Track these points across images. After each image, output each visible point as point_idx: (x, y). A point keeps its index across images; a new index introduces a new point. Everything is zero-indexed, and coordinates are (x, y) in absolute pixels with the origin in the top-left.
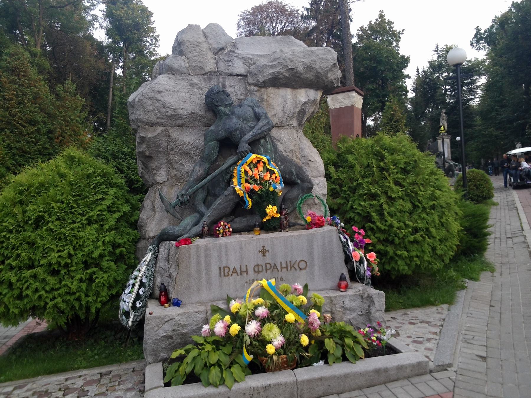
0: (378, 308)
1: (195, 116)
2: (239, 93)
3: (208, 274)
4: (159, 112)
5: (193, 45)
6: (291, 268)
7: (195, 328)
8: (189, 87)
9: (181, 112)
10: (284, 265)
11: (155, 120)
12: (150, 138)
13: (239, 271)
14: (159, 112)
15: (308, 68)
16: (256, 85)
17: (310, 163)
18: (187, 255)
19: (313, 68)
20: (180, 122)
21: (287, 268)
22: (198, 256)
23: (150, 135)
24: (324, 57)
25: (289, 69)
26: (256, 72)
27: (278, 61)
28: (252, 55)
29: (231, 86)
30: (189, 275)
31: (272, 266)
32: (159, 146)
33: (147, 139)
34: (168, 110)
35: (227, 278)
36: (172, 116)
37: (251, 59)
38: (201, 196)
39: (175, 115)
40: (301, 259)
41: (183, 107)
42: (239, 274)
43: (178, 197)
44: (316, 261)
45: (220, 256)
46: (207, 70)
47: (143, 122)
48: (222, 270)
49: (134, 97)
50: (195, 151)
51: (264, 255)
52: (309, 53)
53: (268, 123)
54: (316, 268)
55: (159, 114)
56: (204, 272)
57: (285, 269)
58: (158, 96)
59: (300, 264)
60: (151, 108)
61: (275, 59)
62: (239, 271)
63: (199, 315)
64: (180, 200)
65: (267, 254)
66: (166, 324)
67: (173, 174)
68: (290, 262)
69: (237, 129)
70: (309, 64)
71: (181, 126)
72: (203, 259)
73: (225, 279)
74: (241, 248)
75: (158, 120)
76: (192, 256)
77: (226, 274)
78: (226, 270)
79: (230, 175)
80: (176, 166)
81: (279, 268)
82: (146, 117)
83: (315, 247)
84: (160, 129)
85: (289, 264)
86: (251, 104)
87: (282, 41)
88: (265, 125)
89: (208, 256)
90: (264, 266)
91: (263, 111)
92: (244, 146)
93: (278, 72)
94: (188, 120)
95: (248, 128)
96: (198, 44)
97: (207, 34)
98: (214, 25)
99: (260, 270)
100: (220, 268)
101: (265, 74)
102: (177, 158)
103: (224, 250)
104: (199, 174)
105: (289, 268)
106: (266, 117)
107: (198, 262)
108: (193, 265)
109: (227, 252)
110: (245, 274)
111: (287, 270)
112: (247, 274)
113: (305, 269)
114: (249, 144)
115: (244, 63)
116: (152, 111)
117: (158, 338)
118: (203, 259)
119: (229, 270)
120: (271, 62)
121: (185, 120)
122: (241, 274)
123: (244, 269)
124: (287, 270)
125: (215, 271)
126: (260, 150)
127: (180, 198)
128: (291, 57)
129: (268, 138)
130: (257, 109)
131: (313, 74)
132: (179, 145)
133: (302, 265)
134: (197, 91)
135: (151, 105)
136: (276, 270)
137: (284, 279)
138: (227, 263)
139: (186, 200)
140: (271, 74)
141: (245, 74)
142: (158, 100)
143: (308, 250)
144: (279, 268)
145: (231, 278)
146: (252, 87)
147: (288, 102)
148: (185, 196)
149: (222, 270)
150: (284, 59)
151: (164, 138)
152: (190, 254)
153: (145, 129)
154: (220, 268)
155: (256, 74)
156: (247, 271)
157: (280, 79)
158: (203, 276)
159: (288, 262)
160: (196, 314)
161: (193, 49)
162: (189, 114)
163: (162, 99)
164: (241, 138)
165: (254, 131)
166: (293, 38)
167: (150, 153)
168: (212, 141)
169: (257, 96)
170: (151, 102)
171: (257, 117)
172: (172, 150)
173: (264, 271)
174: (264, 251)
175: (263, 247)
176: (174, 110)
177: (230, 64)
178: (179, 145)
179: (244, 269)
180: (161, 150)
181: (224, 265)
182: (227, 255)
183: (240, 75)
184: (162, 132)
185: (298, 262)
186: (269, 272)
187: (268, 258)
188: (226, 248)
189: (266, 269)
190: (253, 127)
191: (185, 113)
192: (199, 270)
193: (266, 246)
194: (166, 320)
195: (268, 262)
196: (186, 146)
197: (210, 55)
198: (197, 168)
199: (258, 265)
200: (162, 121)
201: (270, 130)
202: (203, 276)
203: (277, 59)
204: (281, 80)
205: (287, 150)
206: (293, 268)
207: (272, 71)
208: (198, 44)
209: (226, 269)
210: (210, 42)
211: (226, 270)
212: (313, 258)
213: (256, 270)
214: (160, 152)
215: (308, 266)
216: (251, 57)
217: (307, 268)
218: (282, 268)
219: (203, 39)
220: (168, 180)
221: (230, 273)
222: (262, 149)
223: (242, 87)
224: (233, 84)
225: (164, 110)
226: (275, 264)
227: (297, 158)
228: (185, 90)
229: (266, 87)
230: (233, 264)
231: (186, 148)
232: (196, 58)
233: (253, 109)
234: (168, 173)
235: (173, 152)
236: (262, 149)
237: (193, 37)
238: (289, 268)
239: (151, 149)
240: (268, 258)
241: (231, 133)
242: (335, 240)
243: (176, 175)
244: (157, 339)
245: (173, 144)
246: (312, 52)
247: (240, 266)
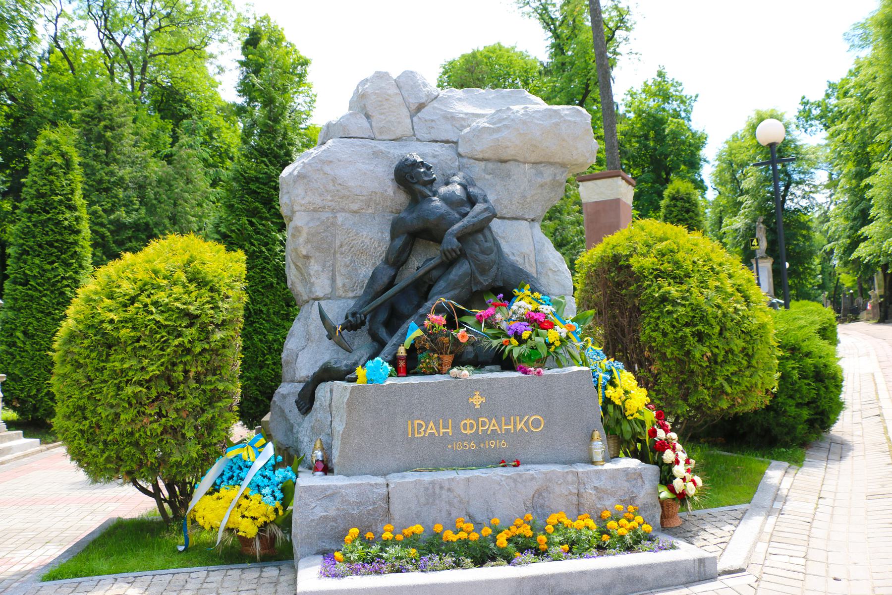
5: (380, 99)
7: (371, 508)
9: (358, 192)
11: (318, 201)
17: (550, 273)
20: (355, 207)
25: (520, 134)
27: (504, 123)
28: (466, 114)
34: (339, 187)
37: (463, 119)
38: (383, 316)
39: (349, 197)
43: (347, 317)
46: (399, 133)
49: (291, 170)
50: (375, 248)
53: (486, 210)
58: (327, 169)
61: (501, 120)
64: (350, 321)
69: (442, 217)
79: (427, 286)
84: (324, 216)
86: (464, 182)
87: (510, 97)
88: (482, 212)
91: (480, 192)
92: (451, 242)
95: (457, 216)
97: (402, 84)
98: (412, 72)
106: (485, 201)
114: (459, 239)
117: (316, 518)
120: (494, 124)
127: (350, 318)
128: (524, 118)
129: (486, 232)
130: (471, 189)
139: (359, 321)
141: (455, 140)
150: (513, 120)
157: (507, 147)
163: (330, 172)
164: (446, 231)
165: (466, 220)
166: (527, 93)
171: (471, 201)
177: (433, 124)
183: (447, 142)
184: (328, 218)
190: (466, 214)
191: (365, 193)
194: (328, 493)
196: (363, 242)
197: (405, 112)
201: (489, 219)
203: (504, 119)
205: (515, 252)
207: (495, 136)
210: (406, 95)
219: (393, 90)
227: (531, 265)
232: (383, 117)
244: (313, 521)
246: (555, 111)
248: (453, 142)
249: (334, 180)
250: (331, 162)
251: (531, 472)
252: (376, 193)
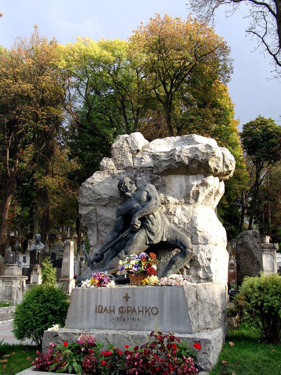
0: (204, 351)
1: (114, 199)
2: (145, 181)
3: (88, 310)
4: (91, 197)
6: (146, 312)
8: (112, 179)
9: (104, 196)
10: (141, 309)
11: (88, 202)
12: (84, 214)
13: (108, 310)
14: (91, 197)
15: (192, 160)
16: (158, 174)
18: (76, 295)
19: (196, 160)
20: (104, 203)
21: (143, 311)
22: (83, 296)
23: (85, 213)
24: (205, 151)
26: (157, 165)
28: (160, 152)
29: (140, 176)
30: (76, 308)
31: (132, 308)
32: (91, 220)
33: (83, 215)
35: (100, 314)
36: (99, 199)
37: (158, 156)
39: (101, 199)
40: (154, 306)
41: (106, 193)
42: (109, 312)
44: (165, 309)
45: (97, 298)
46: (126, 166)
47: (81, 204)
48: (98, 308)
51: (127, 300)
52: (194, 149)
54: (165, 314)
55: (91, 198)
56: (86, 308)
57: (142, 313)
59: (153, 309)
60: (86, 194)
62: (108, 310)
63: (74, 336)
65: (129, 300)
66: (55, 337)
67: (100, 239)
68: (146, 307)
70: (193, 158)
71: (105, 206)
72: (85, 299)
73: (99, 315)
74: (111, 294)
75: (90, 202)
76: (79, 295)
77: (100, 311)
78: (100, 308)
80: (102, 234)
81: (137, 311)
82: (83, 201)
83: (165, 298)
84: (91, 208)
85: (144, 309)
89: (89, 297)
90: (126, 308)
93: (170, 165)
94: (110, 201)
96: (121, 149)
99: (123, 311)
100: (96, 306)
101: (162, 167)
102: (103, 228)
103: (99, 294)
104: (110, 240)
105: (144, 312)
107: (83, 300)
108: (79, 302)
109: (101, 295)
110: (113, 312)
111: (143, 314)
112: (114, 313)
113: (156, 314)
115: (153, 159)
116: (86, 196)
118: (85, 299)
119: (102, 309)
121: (107, 202)
122: (110, 313)
123: (112, 309)
124: (143, 314)
125: (93, 308)
126: (148, 223)
131: (197, 165)
132: (104, 219)
133: (155, 311)
134: (116, 181)
135: (86, 192)
136: (134, 313)
137: (140, 320)
138: (101, 303)
140: (166, 166)
141: (153, 166)
142: (90, 189)
143: (159, 299)
144: (137, 311)
145: (104, 314)
146: (156, 176)
147: (183, 185)
148: (98, 255)
149: (98, 308)
151: (94, 215)
152: (78, 295)
153: (82, 208)
154: (96, 306)
155: (158, 167)
156: (114, 311)
157: (172, 169)
158: (85, 310)
159: (144, 307)
160: (72, 334)
161: (118, 152)
162: (110, 198)
163: (92, 188)
167: (86, 225)
168: (119, 216)
169: (158, 182)
170: (86, 191)
172: (99, 222)
173: (126, 312)
174: (127, 298)
175: (127, 294)
176: (100, 195)
177: (143, 160)
178: (104, 219)
179: (112, 309)
180: (92, 222)
181: (99, 304)
182: (101, 297)
184: (92, 210)
185: (151, 308)
186: (130, 313)
187: (130, 303)
188: (101, 292)
189: (128, 312)
191: (107, 197)
192: (83, 306)
193: (128, 293)
195: (129, 306)
197: (130, 155)
198: (109, 236)
199: (122, 307)
200: (93, 203)
202: (85, 310)
204: (173, 171)
206: (147, 313)
208: (121, 149)
209: (100, 307)
211: (100, 307)
212: (163, 306)
213: (121, 311)
214: (92, 223)
215: (159, 312)
216: (158, 154)
217: (158, 314)
218: (139, 311)
220: (97, 244)
221: (103, 311)
222: (150, 223)
223: (148, 177)
224: (142, 175)
225: (94, 195)
226: (134, 308)
228: (109, 181)
229: (166, 175)
230: (105, 304)
231: (107, 221)
233: (148, 193)
234: (97, 239)
235: (100, 224)
236: (150, 223)
237: (119, 144)
238: (144, 312)
239: (85, 222)
240: (130, 303)
241: (129, 211)
242: (181, 294)
243: (101, 240)
244: (47, 347)
245: (99, 218)
247: (110, 306)
248: (153, 168)
249: (94, 192)
250: (93, 183)
251: (144, 335)
252: (113, 197)
